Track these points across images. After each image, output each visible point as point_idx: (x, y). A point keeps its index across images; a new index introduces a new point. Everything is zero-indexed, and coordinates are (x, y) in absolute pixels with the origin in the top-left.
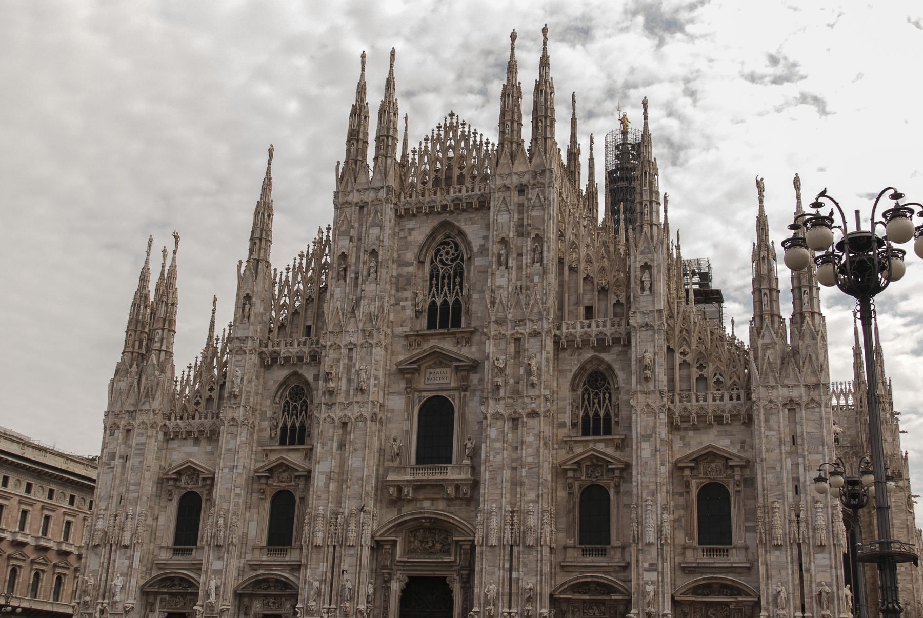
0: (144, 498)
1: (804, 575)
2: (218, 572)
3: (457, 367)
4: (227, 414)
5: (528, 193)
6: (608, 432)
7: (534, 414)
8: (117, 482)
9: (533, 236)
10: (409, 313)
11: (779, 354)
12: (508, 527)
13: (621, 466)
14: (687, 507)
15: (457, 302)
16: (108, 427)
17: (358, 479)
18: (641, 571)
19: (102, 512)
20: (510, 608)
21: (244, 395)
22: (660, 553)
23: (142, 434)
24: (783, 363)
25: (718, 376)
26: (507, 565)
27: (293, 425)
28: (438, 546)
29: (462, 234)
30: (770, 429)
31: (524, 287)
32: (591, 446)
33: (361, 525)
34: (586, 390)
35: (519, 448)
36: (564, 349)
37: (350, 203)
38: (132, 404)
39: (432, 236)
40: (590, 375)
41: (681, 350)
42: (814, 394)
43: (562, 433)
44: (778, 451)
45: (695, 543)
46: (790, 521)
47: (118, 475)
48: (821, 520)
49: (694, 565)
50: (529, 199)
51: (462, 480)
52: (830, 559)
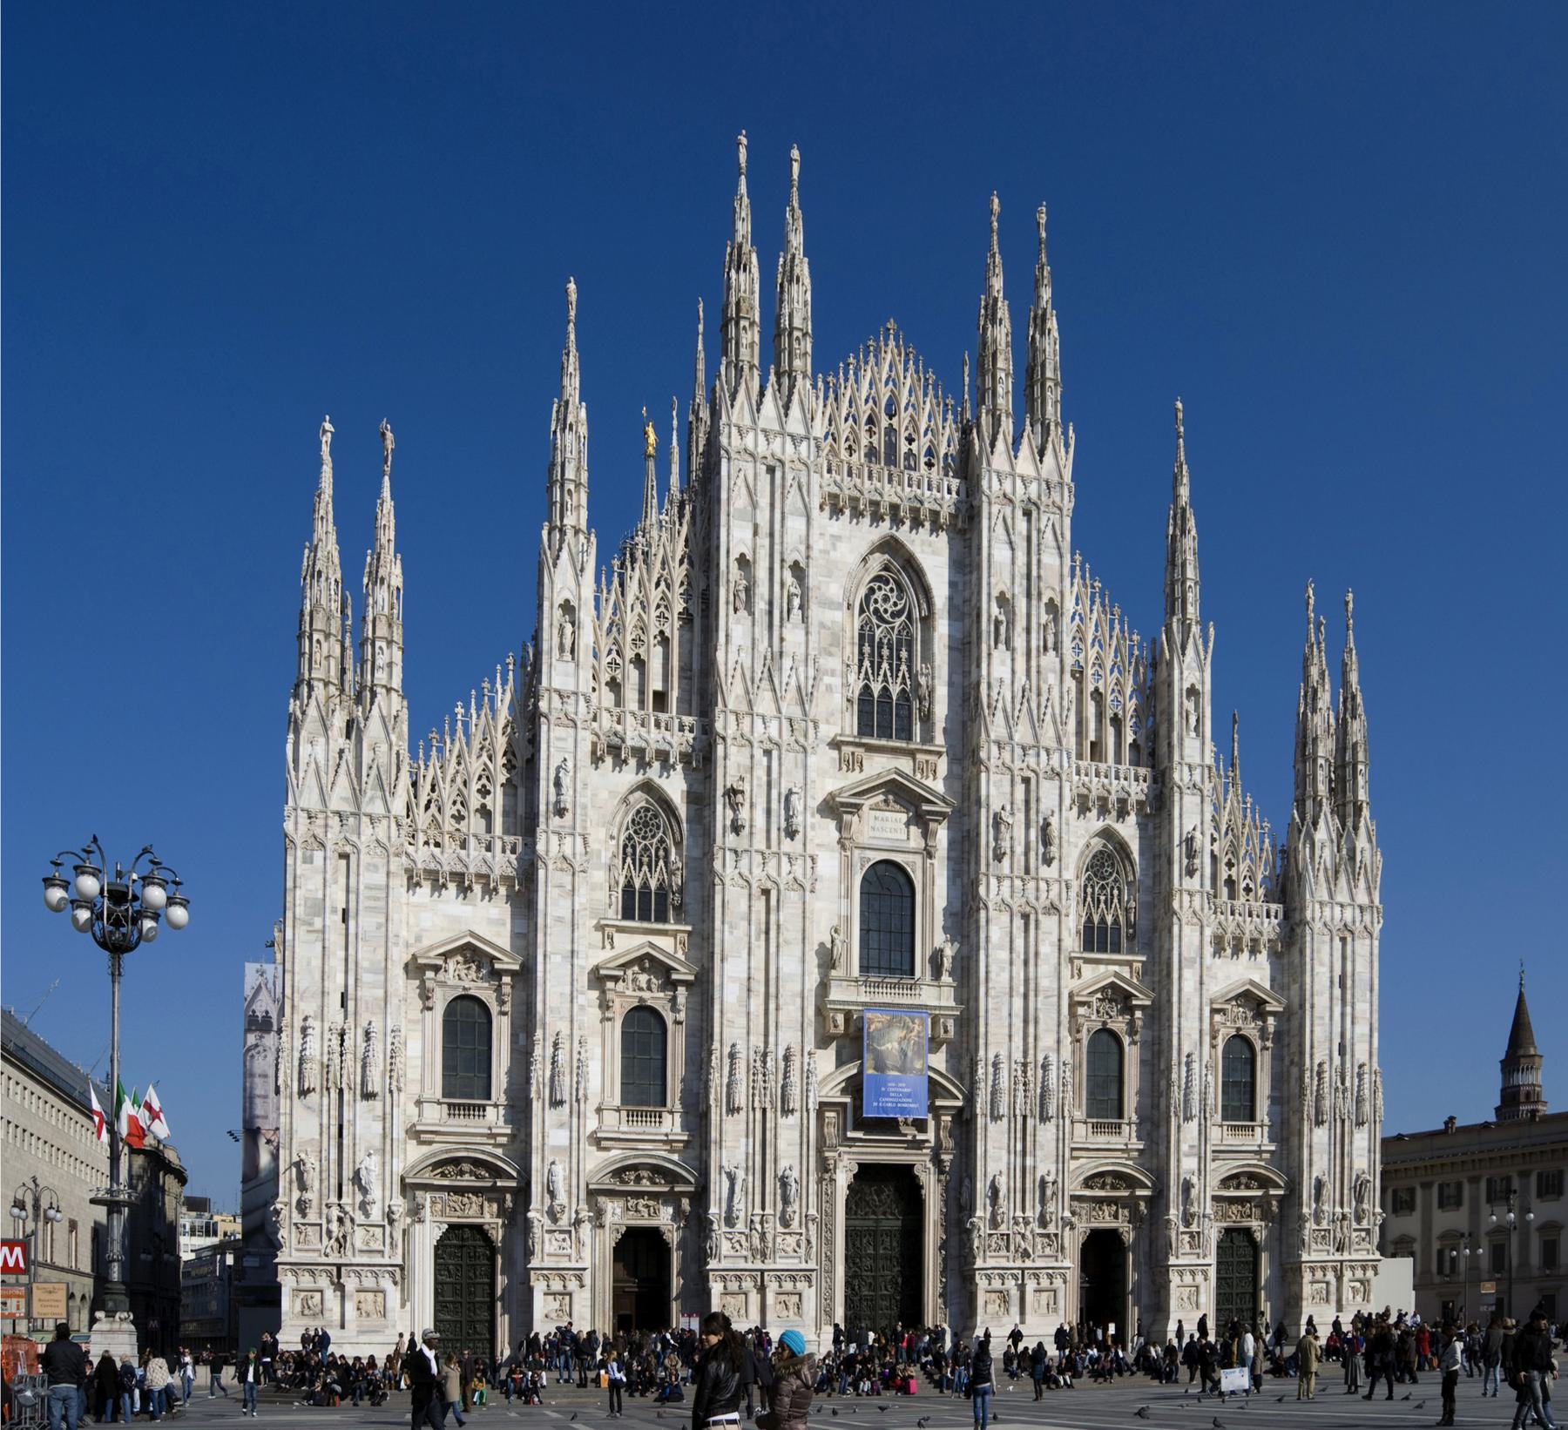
4: (546, 843)
7: (1053, 909)
9: (1045, 599)
12: (1021, 1087)
16: (298, 842)
19: (310, 1022)
21: (578, 811)
22: (1203, 1133)
30: (1322, 964)
33: (807, 1074)
35: (1032, 962)
37: (751, 455)
38: (345, 799)
44: (1327, 995)
46: (1337, 1089)
50: (1039, 531)
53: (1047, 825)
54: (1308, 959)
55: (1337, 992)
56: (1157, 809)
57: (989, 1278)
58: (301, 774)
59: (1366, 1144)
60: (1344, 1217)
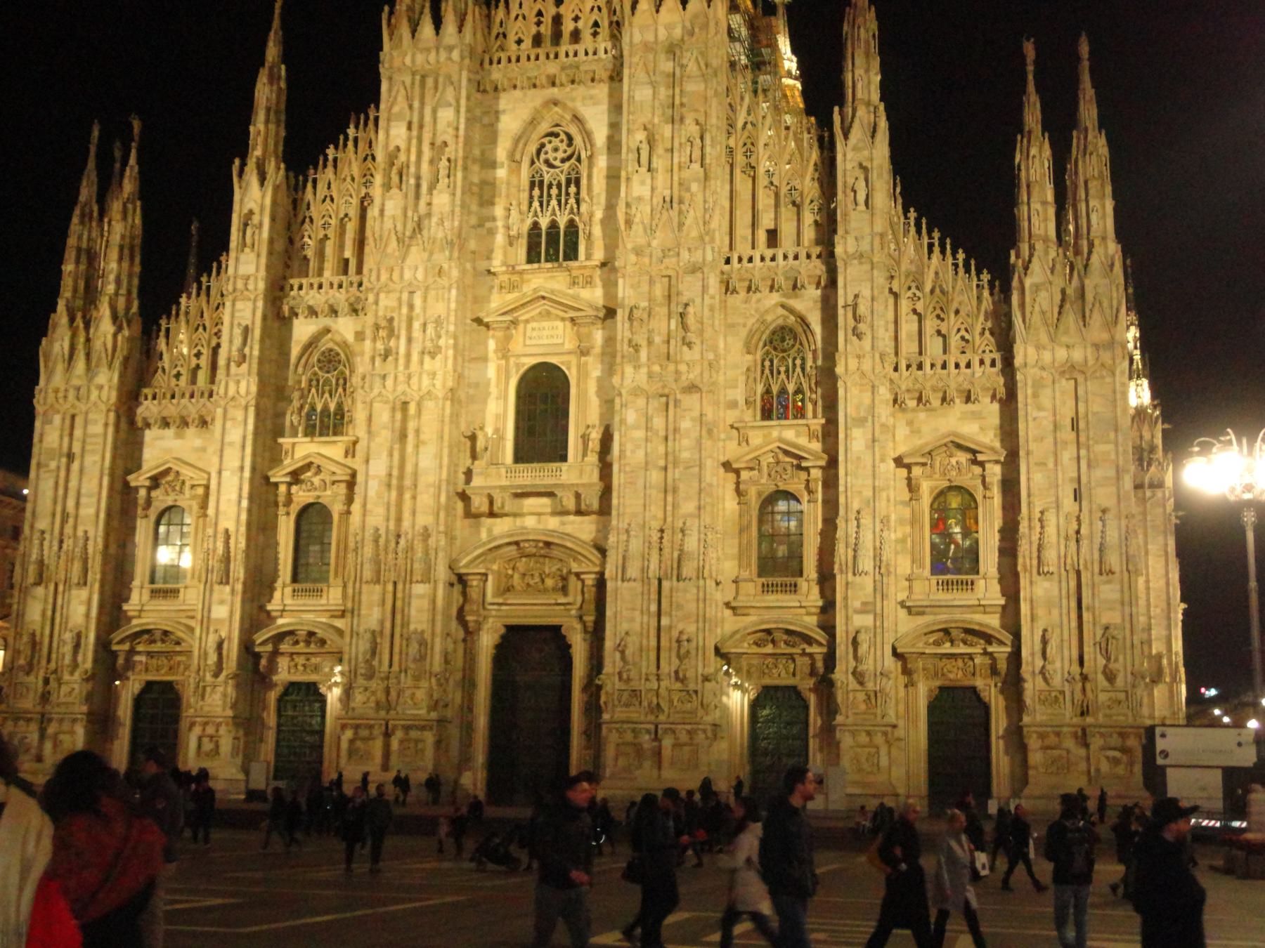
0: (102, 515)
1: (1085, 615)
2: (220, 621)
3: (572, 320)
5: (681, 57)
6: (800, 413)
7: (692, 388)
8: (61, 492)
10: (500, 239)
11: (1058, 297)
13: (823, 463)
14: (914, 521)
15: (572, 224)
17: (428, 486)
18: (850, 611)
20: (658, 667)
22: (880, 590)
23: (96, 422)
24: (1060, 313)
25: (963, 332)
26: (654, 608)
27: (325, 409)
28: (549, 582)
29: (577, 119)
30: (1040, 408)
31: (675, 200)
32: (775, 434)
34: (767, 353)
35: (671, 437)
36: (735, 291)
38: (79, 377)
39: (533, 122)
40: (774, 333)
41: (909, 294)
42: (1106, 356)
43: (731, 416)
44: (1051, 440)
45: (927, 571)
46: (1067, 538)
47: (62, 482)
48: (1113, 536)
49: (925, 603)
50: (682, 66)
51: (583, 485)
52: (1122, 591)
53: (682, 315)
54: (1020, 405)
55: (1067, 434)
56: (832, 283)
57: (617, 730)
58: (50, 364)
59: (1117, 596)
60: (1085, 678)
